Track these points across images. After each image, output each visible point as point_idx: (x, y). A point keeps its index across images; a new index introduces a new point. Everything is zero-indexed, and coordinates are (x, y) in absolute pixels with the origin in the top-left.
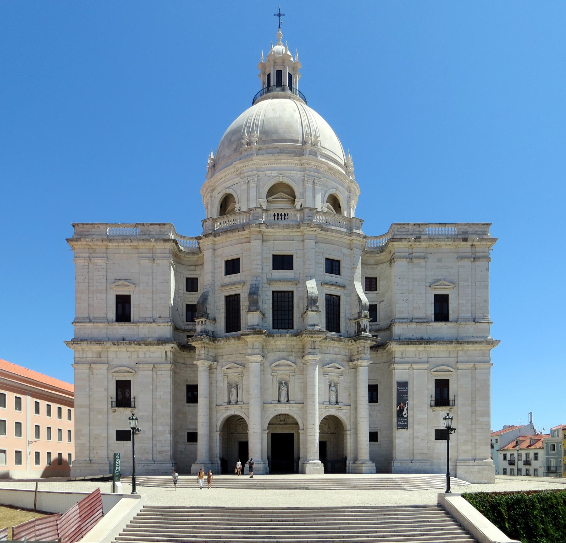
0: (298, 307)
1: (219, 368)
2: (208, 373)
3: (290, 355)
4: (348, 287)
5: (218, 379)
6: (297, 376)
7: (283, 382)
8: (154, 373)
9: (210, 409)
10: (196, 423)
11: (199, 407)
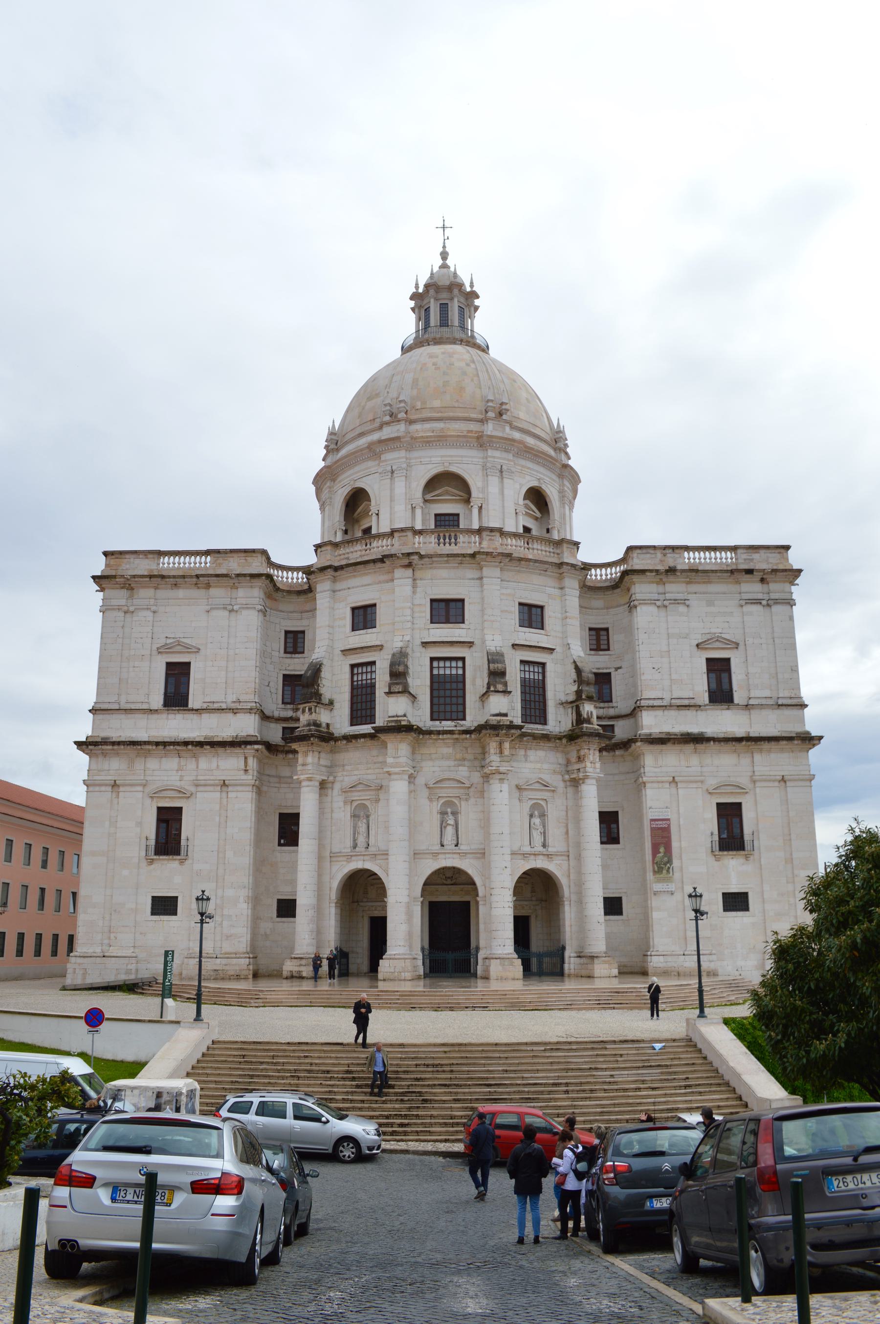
0: (474, 684)
1: (337, 786)
3: (459, 766)
4: (558, 649)
6: (472, 801)
7: (449, 810)
8: (224, 795)
10: (293, 882)
11: (299, 855)
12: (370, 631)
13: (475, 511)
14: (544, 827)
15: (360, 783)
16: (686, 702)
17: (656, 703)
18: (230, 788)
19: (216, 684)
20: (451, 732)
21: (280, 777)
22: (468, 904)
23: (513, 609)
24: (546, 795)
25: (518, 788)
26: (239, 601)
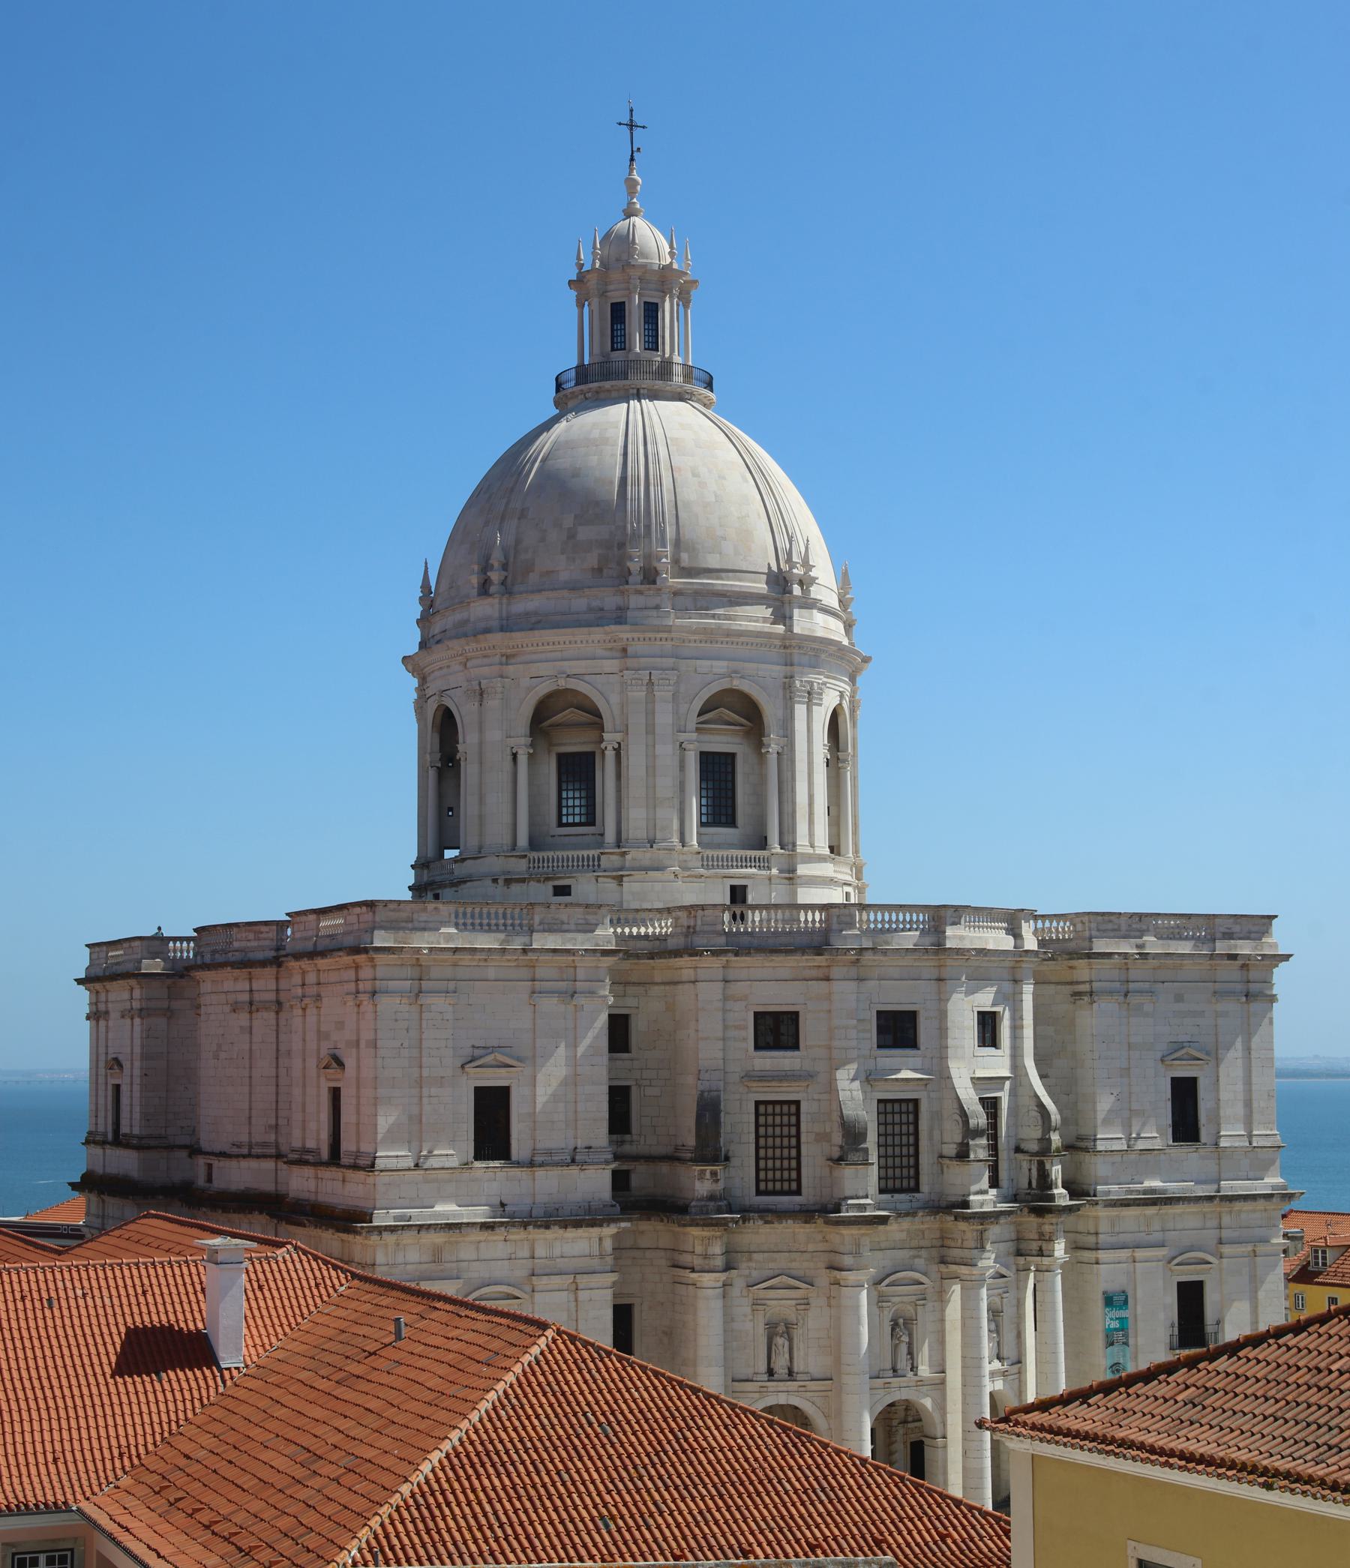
0: (931, 1138)
6: (930, 1305)
7: (901, 1321)
12: (789, 1053)
13: (772, 758)
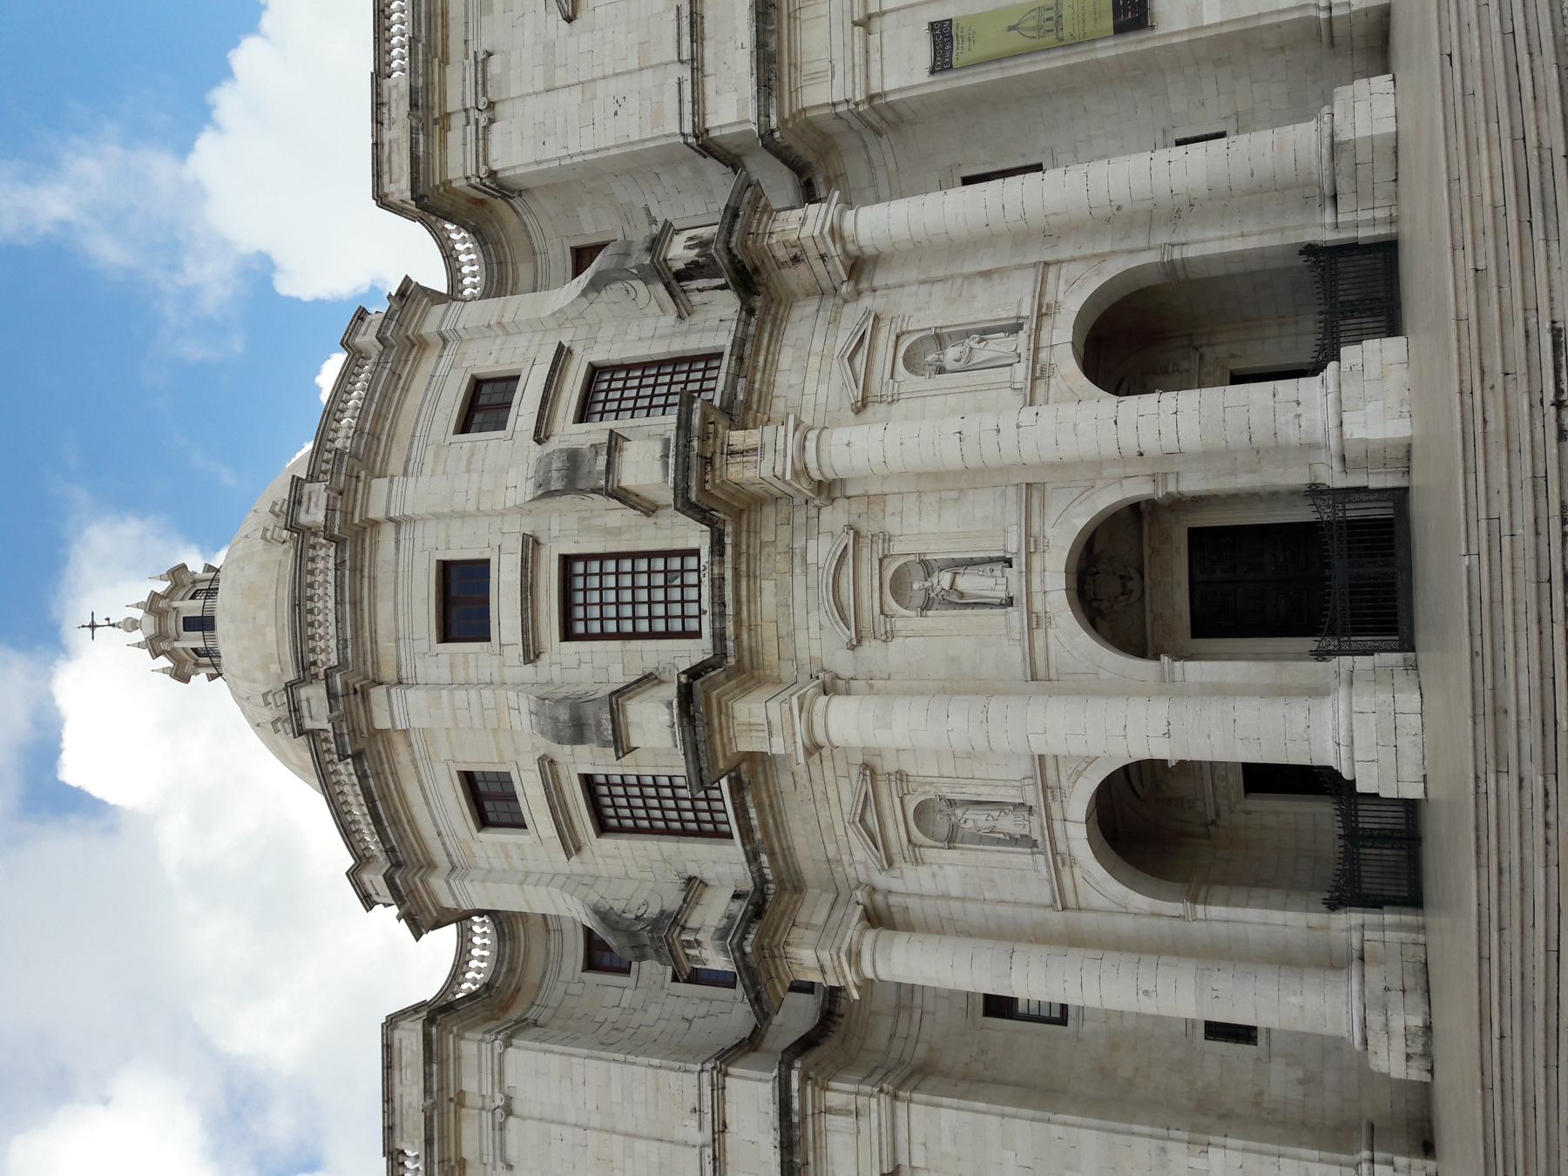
1: (881, 880)
2: (901, 938)
5: (929, 887)
6: (892, 525)
9: (1073, 940)
14: (967, 334)
15: (862, 820)
16: (686, 23)
17: (687, 96)
18: (903, 1160)
19: (661, 1164)
20: (718, 584)
21: (899, 1007)
22: (1196, 535)
23: (466, 446)
24: (885, 338)
25: (861, 407)
26: (487, 1091)
